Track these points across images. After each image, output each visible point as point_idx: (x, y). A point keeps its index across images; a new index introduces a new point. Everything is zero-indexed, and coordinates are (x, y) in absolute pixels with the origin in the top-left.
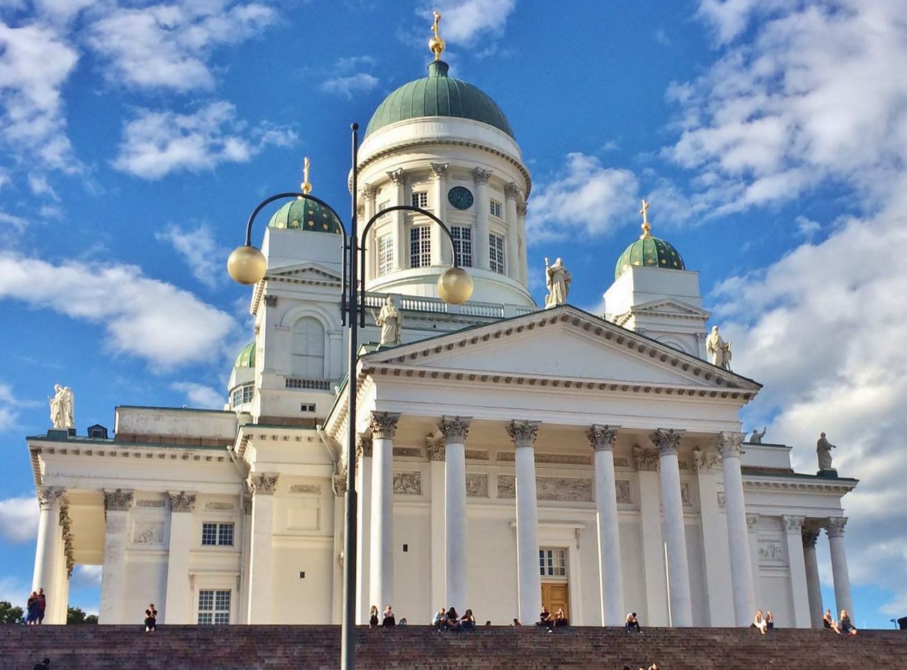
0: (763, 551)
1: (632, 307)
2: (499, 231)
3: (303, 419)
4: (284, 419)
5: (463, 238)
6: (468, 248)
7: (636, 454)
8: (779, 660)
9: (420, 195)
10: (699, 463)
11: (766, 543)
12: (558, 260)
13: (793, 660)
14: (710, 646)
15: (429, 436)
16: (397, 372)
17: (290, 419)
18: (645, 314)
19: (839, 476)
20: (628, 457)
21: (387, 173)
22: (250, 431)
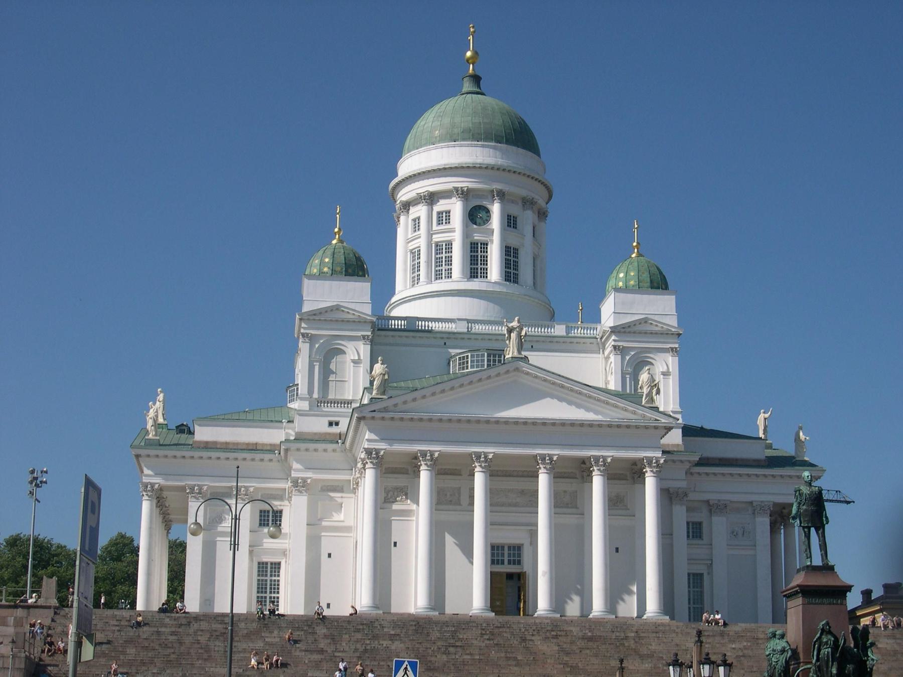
0: (733, 532)
1: (610, 328)
2: (513, 242)
3: (329, 434)
4: (315, 434)
6: (485, 261)
7: (583, 470)
9: (444, 213)
12: (516, 319)
14: (566, 635)
15: (413, 459)
16: (383, 418)
17: (320, 434)
18: (625, 332)
21: (417, 194)
22: (288, 445)
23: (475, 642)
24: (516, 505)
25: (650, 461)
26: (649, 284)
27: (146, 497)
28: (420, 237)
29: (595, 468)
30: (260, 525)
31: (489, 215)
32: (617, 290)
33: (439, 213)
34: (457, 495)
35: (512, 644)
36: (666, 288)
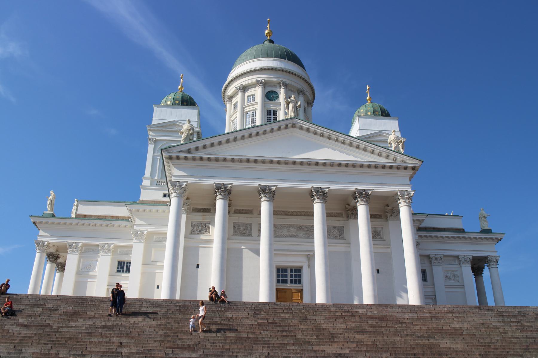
3: (163, 202)
5: (273, 115)
7: (347, 209)
8: (404, 325)
9: (251, 96)
10: (389, 215)
11: (450, 272)
13: (417, 325)
14: (353, 315)
16: (186, 158)
19: (493, 232)
20: (343, 212)
21: (235, 88)
23: (245, 321)
24: (295, 236)
25: (403, 193)
26: (380, 114)
27: (38, 251)
28: (237, 112)
29: (359, 199)
30: (118, 271)
31: (277, 95)
32: (360, 116)
33: (248, 97)
34: (249, 229)
35: (290, 323)
36: (390, 116)
